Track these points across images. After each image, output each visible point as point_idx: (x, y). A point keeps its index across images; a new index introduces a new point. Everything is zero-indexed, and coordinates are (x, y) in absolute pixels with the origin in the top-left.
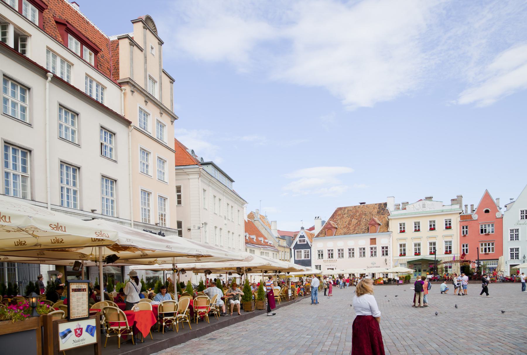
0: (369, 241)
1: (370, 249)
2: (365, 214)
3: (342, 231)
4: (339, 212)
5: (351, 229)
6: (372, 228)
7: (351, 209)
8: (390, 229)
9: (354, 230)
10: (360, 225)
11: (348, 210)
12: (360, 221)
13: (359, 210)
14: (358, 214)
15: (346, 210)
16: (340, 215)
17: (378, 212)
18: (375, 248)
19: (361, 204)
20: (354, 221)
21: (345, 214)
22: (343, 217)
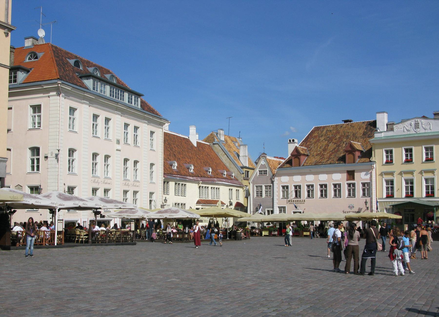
0: (345, 175)
1: (346, 186)
2: (347, 137)
3: (314, 160)
4: (316, 134)
5: (326, 157)
6: (349, 157)
7: (331, 129)
8: (373, 159)
9: (329, 158)
10: (338, 151)
11: (327, 131)
12: (339, 146)
13: (341, 130)
14: (338, 136)
15: (325, 131)
16: (316, 137)
17: (364, 134)
18: (354, 185)
19: (346, 121)
20: (332, 146)
21: (322, 136)
22: (319, 140)
